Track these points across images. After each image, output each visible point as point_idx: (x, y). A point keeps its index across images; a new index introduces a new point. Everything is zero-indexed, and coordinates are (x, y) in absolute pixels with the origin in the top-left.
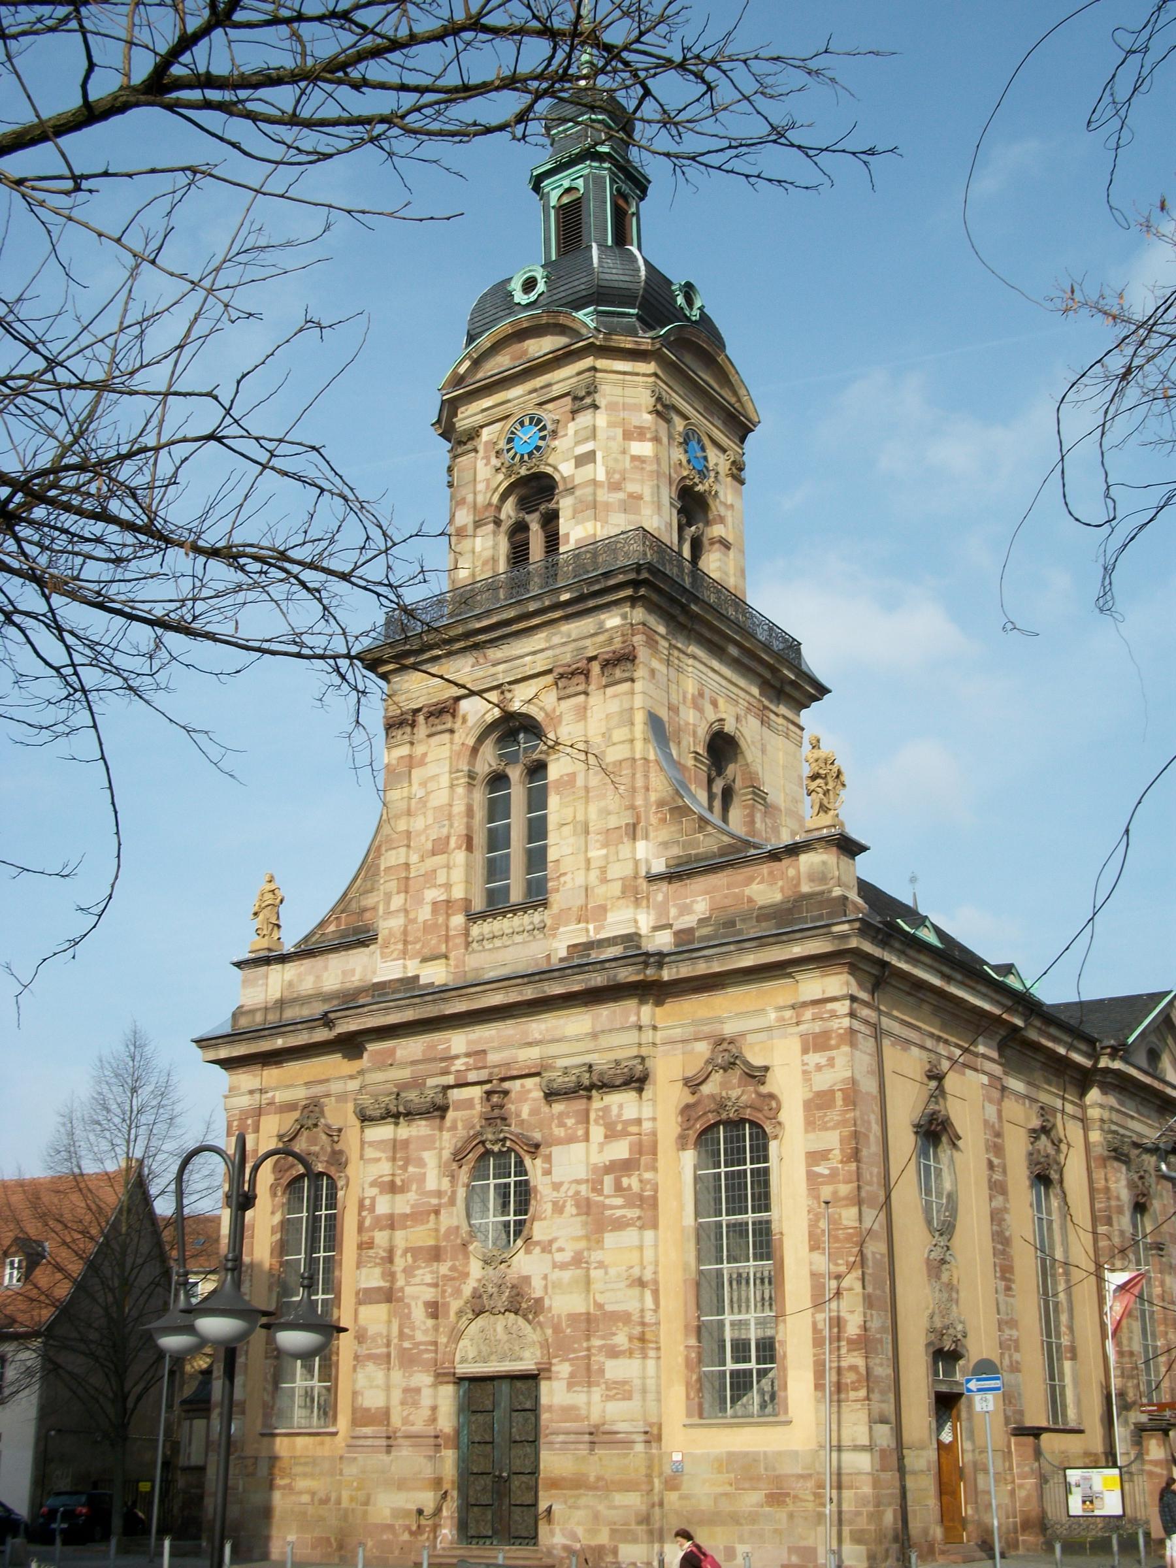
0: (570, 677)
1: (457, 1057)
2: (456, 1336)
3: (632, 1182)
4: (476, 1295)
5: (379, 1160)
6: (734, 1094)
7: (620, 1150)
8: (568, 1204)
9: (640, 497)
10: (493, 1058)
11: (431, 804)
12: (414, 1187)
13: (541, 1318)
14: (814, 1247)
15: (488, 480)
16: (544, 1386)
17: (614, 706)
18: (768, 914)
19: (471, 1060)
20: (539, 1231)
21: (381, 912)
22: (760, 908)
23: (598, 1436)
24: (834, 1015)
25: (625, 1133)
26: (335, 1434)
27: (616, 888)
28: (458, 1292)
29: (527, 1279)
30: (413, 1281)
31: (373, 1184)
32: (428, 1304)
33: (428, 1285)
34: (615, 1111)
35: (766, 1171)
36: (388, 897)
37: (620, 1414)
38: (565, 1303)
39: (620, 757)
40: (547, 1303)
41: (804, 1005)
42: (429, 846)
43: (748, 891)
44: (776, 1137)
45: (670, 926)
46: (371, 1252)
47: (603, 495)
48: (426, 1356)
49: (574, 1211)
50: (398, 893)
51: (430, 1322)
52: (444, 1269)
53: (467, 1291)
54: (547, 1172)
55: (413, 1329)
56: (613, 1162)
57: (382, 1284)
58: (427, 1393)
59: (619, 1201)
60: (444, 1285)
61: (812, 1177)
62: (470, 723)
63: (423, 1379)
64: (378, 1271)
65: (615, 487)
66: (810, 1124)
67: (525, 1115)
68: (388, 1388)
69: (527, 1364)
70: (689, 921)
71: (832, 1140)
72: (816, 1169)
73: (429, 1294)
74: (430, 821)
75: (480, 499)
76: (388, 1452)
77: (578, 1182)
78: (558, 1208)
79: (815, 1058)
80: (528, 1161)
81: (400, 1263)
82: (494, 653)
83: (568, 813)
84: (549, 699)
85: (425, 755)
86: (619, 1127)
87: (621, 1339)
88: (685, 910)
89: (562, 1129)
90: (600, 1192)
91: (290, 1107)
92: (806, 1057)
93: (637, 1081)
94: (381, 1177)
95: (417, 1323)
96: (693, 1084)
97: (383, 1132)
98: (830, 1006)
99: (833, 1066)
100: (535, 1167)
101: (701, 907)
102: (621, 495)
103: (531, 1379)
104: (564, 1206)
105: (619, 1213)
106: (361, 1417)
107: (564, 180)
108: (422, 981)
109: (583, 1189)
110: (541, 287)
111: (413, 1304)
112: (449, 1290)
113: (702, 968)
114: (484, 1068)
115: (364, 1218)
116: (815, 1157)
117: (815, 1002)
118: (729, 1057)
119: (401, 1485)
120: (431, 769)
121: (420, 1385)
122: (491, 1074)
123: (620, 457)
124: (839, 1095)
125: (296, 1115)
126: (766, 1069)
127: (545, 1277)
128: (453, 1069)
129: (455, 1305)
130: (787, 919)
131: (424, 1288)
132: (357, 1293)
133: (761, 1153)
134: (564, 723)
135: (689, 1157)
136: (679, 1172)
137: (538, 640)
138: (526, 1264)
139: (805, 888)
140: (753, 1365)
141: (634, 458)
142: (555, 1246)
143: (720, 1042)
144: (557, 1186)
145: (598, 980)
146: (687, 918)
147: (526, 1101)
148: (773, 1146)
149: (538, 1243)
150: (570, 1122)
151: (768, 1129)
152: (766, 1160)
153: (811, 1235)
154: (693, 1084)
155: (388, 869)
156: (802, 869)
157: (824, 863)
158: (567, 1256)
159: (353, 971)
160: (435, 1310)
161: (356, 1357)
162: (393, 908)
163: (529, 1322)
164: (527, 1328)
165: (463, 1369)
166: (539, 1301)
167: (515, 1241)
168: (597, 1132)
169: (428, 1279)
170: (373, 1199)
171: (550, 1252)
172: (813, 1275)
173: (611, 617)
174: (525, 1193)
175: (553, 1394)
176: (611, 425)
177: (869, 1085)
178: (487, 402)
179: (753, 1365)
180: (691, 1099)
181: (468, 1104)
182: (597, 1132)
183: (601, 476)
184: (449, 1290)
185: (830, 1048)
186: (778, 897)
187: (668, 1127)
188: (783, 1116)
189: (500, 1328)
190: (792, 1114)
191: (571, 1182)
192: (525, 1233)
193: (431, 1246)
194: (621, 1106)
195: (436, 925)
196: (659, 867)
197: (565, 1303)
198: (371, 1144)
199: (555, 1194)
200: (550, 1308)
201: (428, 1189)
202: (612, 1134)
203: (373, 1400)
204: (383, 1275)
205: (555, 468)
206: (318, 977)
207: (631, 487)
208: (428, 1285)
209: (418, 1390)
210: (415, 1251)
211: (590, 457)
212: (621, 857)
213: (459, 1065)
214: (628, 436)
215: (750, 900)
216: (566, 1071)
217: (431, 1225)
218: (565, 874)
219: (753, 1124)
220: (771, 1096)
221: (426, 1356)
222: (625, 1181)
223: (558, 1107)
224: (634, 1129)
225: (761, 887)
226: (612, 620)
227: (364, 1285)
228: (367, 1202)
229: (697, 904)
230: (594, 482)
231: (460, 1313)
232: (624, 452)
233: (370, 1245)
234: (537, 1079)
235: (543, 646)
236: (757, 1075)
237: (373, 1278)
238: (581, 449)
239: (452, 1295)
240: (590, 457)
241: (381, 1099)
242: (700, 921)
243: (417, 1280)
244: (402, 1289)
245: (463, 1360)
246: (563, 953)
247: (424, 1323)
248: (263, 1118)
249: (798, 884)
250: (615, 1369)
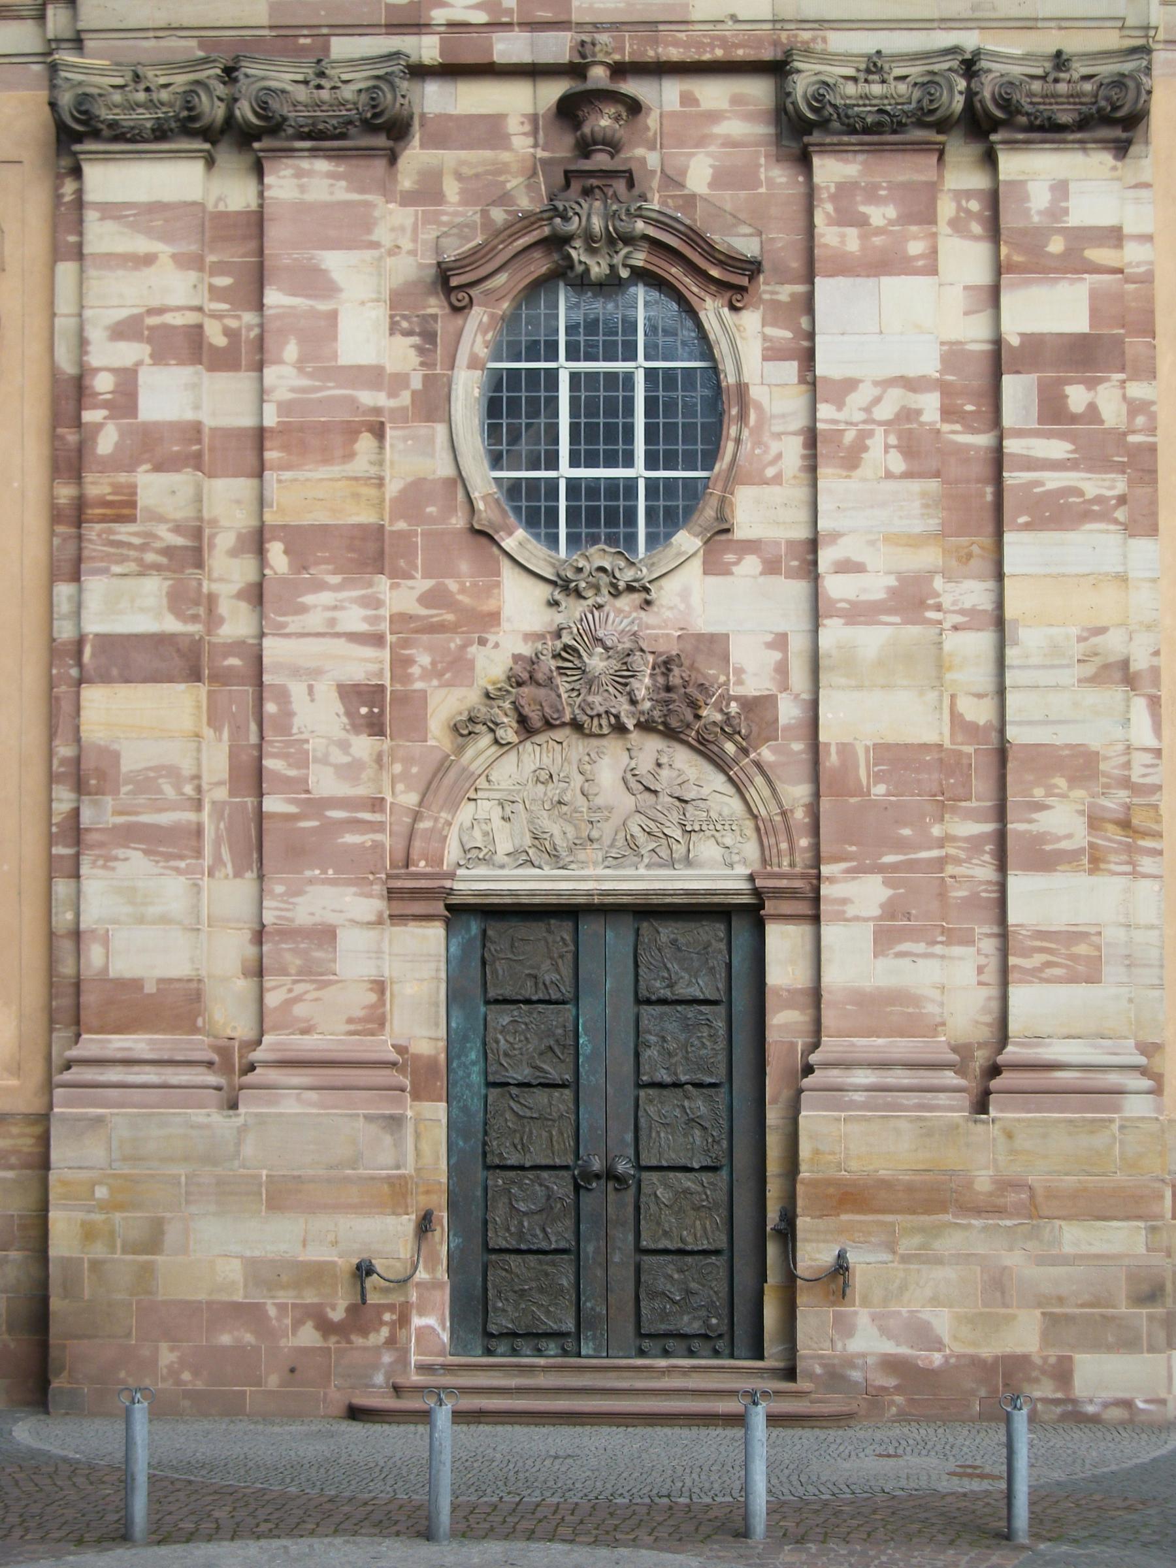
2: (444, 783)
4: (525, 675)
13: (766, 754)
28: (456, 668)
30: (294, 623)
32: (352, 694)
33: (353, 637)
48: (351, 839)
51: (364, 746)
52: (401, 596)
55: (303, 761)
57: (172, 625)
58: (351, 941)
60: (406, 643)
63: (348, 905)
64: (154, 588)
89: (852, 233)
95: (315, 745)
111: (297, 690)
112: (424, 659)
121: (332, 919)
129: (446, 704)
131: (341, 646)
138: (711, 602)
160: (374, 709)
163: (720, 764)
164: (710, 783)
166: (751, 705)
169: (354, 619)
184: (424, 659)
192: (708, 512)
193: (361, 527)
204: (178, 601)
208: (353, 637)
210: (305, 542)
217: (361, 465)
221: (351, 839)
227: (93, 625)
231: (465, 729)
239: (434, 672)
243: (314, 621)
247: (344, 746)
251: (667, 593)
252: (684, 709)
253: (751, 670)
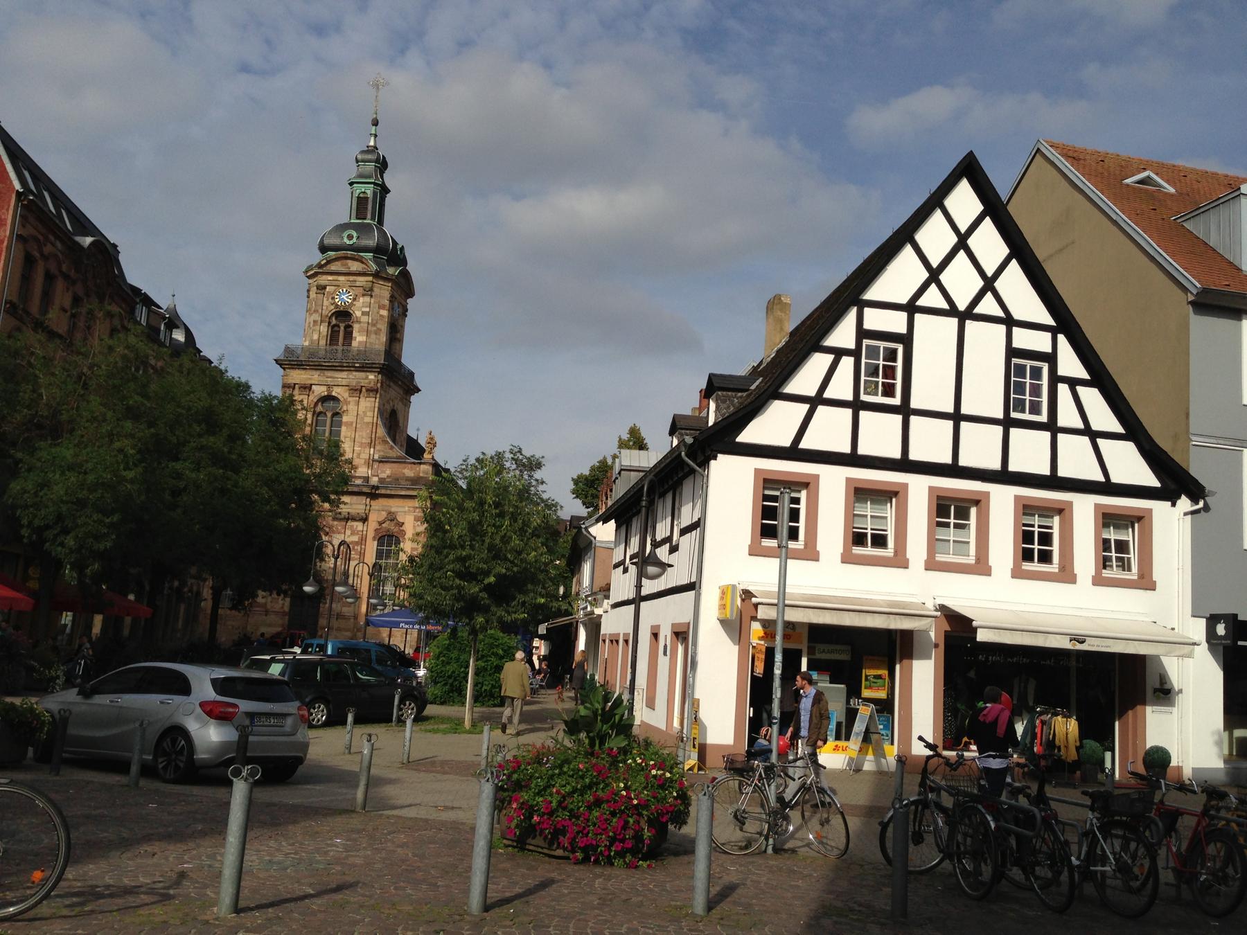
0: (356, 391)
7: (355, 538)
17: (368, 404)
18: (408, 479)
23: (340, 616)
65: (374, 325)
70: (383, 475)
82: (329, 374)
84: (346, 395)
93: (364, 520)
96: (380, 523)
101: (388, 472)
107: (362, 188)
110: (355, 240)
113: (388, 492)
118: (392, 517)
119: (270, 625)
130: (415, 481)
136: (371, 548)
137: (344, 374)
143: (390, 513)
145: (356, 489)
154: (380, 523)
168: (348, 532)
178: (330, 278)
187: (371, 534)
196: (376, 457)
226: (371, 377)
229: (387, 471)
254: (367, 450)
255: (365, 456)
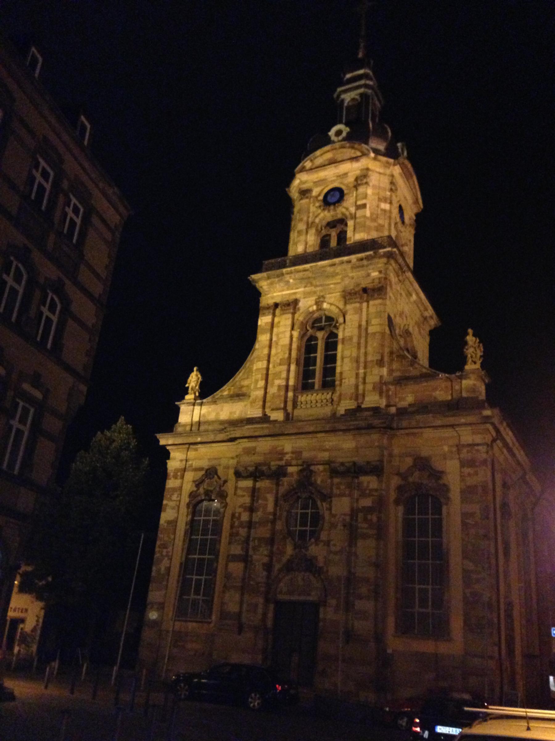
1: (287, 453)
3: (374, 518)
5: (243, 496)
6: (425, 482)
7: (367, 502)
8: (339, 525)
9: (383, 226)
10: (306, 455)
11: (279, 344)
12: (261, 510)
14: (465, 556)
15: (314, 213)
16: (321, 610)
19: (294, 456)
20: (324, 536)
21: (252, 387)
22: (440, 402)
23: (350, 636)
24: (478, 451)
25: (370, 495)
26: (210, 623)
27: (369, 387)
29: (316, 558)
31: (240, 506)
34: (365, 484)
35: (441, 520)
36: (257, 381)
37: (362, 626)
38: (336, 571)
39: (374, 331)
40: (325, 569)
41: (463, 446)
42: (278, 361)
43: (434, 394)
44: (447, 504)
45: (395, 406)
46: (237, 538)
47: (368, 223)
49: (342, 528)
50: (262, 380)
53: (285, 559)
54: (330, 509)
56: (363, 507)
59: (366, 526)
61: (464, 524)
62: (301, 311)
64: (239, 547)
66: (464, 500)
67: (319, 481)
68: (241, 603)
69: (313, 597)
70: (403, 404)
71: (475, 508)
72: (467, 521)
73: (266, 560)
74: (280, 351)
75: (310, 220)
76: (240, 634)
77: (345, 515)
78: (333, 526)
79: (467, 470)
80: (319, 503)
81: (251, 544)
83: (347, 353)
85: (279, 322)
86: (367, 492)
87: (364, 590)
88: (403, 399)
89: (338, 491)
90: (357, 520)
91: (201, 469)
92: (463, 470)
94: (245, 504)
97: (249, 483)
98: (476, 448)
99: (477, 475)
100: (323, 506)
101: (410, 399)
102: (376, 224)
103: (315, 607)
104: (337, 525)
105: (365, 531)
106: (224, 615)
108: (272, 419)
109: (348, 518)
114: (301, 459)
115: (234, 522)
116: (465, 515)
117: (469, 445)
120: (281, 329)
122: (304, 462)
123: (377, 208)
124: (480, 488)
125: (203, 472)
126: (442, 472)
127: (325, 557)
128: (285, 458)
129: (277, 566)
132: (228, 556)
133: (438, 510)
134: (348, 314)
135: (401, 509)
136: (396, 515)
138: (315, 550)
139: (464, 395)
140: (429, 610)
141: (382, 210)
142: (332, 543)
144: (334, 516)
146: (402, 403)
147: (321, 477)
148: (444, 509)
149: (322, 541)
150: (342, 487)
151: (442, 500)
152: (440, 514)
153: (463, 552)
155: (257, 370)
156: (463, 386)
157: (474, 385)
158: (338, 548)
159: (235, 413)
161: (225, 586)
162: (258, 386)
165: (280, 597)
166: (321, 568)
167: (310, 539)
170: (240, 514)
171: (328, 545)
172: (464, 570)
173: (373, 272)
174: (317, 519)
175: (329, 614)
176: (373, 194)
177: (490, 486)
179: (429, 610)
180: (403, 483)
181: (292, 474)
182: (356, 494)
183: (368, 213)
185: (477, 466)
186: (450, 398)
187: (393, 495)
188: (451, 495)
189: (299, 579)
190: (455, 494)
191: (342, 514)
194: (369, 482)
195: (279, 396)
197: (336, 571)
198: (241, 488)
199: (333, 519)
200: (327, 571)
201: (268, 511)
202: (364, 494)
203: (233, 608)
205: (347, 209)
206: (218, 414)
207: (381, 221)
209: (256, 606)
210: (260, 539)
211: (364, 206)
212: (373, 372)
213: (288, 457)
214: (380, 200)
215: (435, 398)
216: (342, 464)
218: (345, 379)
219: (432, 496)
220: (444, 485)
222: (369, 517)
223: (336, 480)
224: (376, 494)
225: (442, 393)
228: (237, 515)
230: (365, 216)
231: (280, 570)
232: (378, 206)
233: (237, 534)
234: (327, 466)
235: (339, 281)
236: (438, 475)
237: (237, 550)
238: (359, 203)
240: (364, 206)
241: (249, 468)
242: (410, 405)
244: (251, 556)
245: (281, 592)
246: (342, 412)
247: (262, 573)
248: (186, 473)
249: (461, 393)
250: (359, 605)
251: (310, 548)
252: (310, 565)
253: (321, 559)
254: (376, 371)
255: (373, 378)
